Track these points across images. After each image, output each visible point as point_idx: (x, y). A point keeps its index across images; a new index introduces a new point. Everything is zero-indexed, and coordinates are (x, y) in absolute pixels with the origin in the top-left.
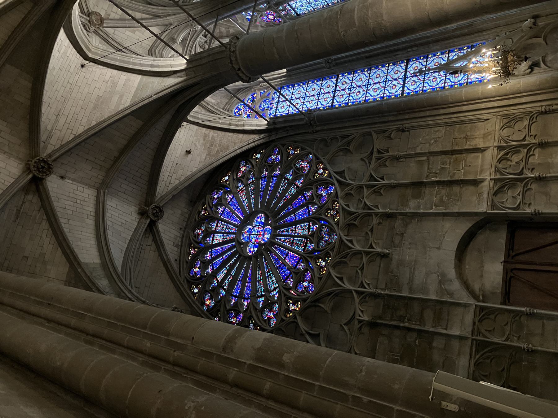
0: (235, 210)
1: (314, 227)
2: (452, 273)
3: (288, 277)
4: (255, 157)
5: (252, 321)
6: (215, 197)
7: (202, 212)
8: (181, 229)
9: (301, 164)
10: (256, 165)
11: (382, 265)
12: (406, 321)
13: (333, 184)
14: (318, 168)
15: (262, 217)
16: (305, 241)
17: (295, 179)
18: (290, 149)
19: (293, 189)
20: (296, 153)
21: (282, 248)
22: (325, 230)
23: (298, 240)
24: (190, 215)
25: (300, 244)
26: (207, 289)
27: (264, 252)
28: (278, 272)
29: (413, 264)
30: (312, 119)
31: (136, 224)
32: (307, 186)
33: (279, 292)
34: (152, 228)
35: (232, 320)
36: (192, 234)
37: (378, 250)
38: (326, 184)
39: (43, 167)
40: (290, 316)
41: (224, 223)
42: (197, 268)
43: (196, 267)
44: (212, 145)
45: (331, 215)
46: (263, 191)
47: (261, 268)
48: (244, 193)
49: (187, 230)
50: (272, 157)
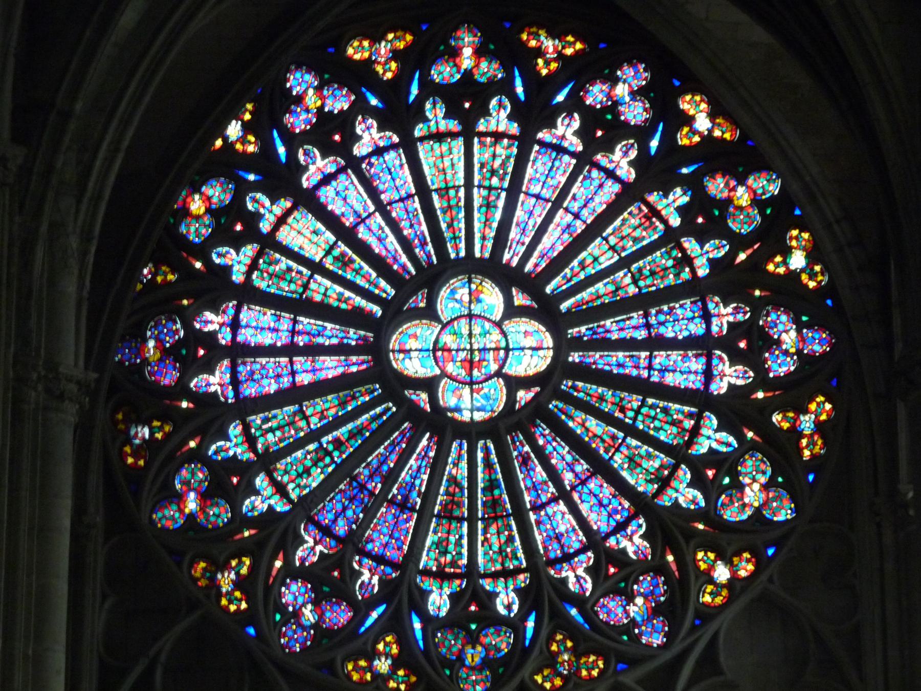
1: (512, 595)
3: (326, 531)
4: (794, 243)
5: (161, 428)
9: (754, 480)
14: (736, 559)
15: (541, 353)
16: (459, 567)
17: (697, 465)
19: (657, 463)
22: (502, 642)
23: (461, 537)
25: (445, 553)
28: (342, 487)
35: (151, 344)
40: (198, 579)
42: (319, 103)
43: (323, 98)
46: (648, 326)
48: (637, 234)
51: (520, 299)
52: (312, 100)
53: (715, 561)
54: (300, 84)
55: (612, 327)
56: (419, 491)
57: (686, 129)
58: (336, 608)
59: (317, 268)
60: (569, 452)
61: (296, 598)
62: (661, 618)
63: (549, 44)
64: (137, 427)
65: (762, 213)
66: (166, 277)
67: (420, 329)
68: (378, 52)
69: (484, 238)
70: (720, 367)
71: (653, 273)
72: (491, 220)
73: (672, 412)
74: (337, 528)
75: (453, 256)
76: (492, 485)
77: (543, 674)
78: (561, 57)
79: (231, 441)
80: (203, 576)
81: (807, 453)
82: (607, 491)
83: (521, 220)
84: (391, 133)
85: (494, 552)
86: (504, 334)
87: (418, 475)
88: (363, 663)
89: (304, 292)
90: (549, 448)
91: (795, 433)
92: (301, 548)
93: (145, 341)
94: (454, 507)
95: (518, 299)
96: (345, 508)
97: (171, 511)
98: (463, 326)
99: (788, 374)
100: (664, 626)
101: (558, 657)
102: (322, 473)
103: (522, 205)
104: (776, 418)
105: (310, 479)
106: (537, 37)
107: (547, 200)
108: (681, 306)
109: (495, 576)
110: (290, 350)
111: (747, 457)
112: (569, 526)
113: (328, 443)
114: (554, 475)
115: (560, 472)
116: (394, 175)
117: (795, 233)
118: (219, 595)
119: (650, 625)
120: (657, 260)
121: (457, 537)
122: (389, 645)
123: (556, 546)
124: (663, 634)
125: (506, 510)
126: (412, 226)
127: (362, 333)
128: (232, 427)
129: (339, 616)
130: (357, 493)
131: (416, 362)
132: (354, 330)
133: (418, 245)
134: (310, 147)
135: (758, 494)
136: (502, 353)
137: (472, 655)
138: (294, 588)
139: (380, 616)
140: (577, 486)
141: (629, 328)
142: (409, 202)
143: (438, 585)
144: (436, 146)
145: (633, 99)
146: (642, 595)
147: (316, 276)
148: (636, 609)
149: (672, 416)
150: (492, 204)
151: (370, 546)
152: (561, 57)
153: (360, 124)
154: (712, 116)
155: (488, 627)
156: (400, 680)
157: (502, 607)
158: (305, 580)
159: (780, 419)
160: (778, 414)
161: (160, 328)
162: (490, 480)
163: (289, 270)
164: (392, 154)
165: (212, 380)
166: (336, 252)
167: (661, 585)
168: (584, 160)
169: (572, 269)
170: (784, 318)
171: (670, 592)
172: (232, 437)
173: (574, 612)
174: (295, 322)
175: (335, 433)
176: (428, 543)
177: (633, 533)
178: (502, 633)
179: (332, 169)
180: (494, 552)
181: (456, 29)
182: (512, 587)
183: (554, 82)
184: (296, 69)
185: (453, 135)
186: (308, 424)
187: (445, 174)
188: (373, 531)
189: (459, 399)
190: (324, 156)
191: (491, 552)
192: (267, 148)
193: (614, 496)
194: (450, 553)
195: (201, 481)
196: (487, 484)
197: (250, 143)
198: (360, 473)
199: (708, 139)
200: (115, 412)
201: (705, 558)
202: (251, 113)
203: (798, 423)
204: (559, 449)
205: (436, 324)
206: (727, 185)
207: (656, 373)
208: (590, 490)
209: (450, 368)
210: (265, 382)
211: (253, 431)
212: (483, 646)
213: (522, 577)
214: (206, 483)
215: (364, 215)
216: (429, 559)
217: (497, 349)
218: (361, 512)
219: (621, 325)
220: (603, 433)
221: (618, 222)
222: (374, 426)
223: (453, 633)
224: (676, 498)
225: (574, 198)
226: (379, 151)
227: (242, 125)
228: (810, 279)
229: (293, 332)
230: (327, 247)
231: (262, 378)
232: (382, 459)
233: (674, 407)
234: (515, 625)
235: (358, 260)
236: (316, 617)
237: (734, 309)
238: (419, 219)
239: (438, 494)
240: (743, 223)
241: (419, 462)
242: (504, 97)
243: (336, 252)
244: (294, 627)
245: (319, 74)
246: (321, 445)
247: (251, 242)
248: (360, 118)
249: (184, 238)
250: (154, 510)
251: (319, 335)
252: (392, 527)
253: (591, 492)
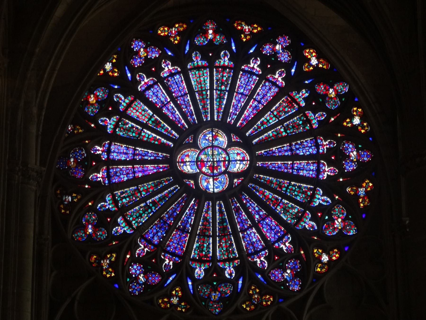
0: (255, 100)
1: (232, 269)
3: (149, 242)
4: (355, 113)
5: (76, 197)
6: (278, 47)
7: (247, 28)
9: (339, 217)
14: (331, 252)
15: (244, 162)
17: (314, 211)
18: (369, 186)
20: (361, 200)
21: (193, 218)
22: (228, 290)
23: (209, 244)
28: (156, 222)
35: (72, 160)
40: (93, 263)
41: (230, 82)
42: (145, 54)
43: (147, 52)
46: (291, 150)
50: (352, 152)
51: (234, 139)
53: (322, 253)
54: (137, 47)
55: (276, 150)
56: (190, 224)
57: (307, 64)
58: (153, 276)
59: (145, 126)
60: (257, 206)
61: (136, 271)
62: (298, 279)
63: (246, 28)
64: (66, 197)
65: (341, 100)
66: (78, 131)
67: (190, 153)
68: (171, 32)
69: (218, 112)
70: (323, 168)
71: (293, 127)
72: (221, 104)
73: (303, 188)
74: (154, 241)
75: (205, 120)
76: (223, 221)
77: (246, 304)
78: (251, 33)
79: (107, 202)
80: (95, 261)
81: (362, 205)
83: (235, 104)
84: (177, 67)
85: (224, 251)
86: (228, 154)
87: (190, 217)
88: (166, 300)
89: (139, 137)
90: (248, 204)
91: (356, 196)
92: (138, 250)
93: (70, 158)
94: (206, 231)
95: (234, 139)
96: (157, 232)
97: (81, 234)
98: (209, 151)
99: (353, 170)
100: (299, 282)
101: (253, 296)
102: (147, 216)
103: (235, 98)
104: (348, 189)
105: (142, 219)
106: (241, 25)
107: (246, 96)
108: (306, 141)
109: (224, 261)
110: (133, 162)
111: (335, 207)
112: (257, 239)
113: (150, 203)
114: (251, 217)
115: (253, 215)
116: (179, 85)
117: (355, 109)
118: (102, 270)
119: (293, 282)
120: (295, 121)
121: (207, 244)
122: (177, 291)
123: (251, 247)
124: (299, 285)
125: (229, 232)
126: (186, 107)
127: (165, 154)
128: (107, 196)
129: (155, 279)
130: (163, 225)
131: (189, 167)
132: (161, 153)
133: (189, 115)
134: (142, 74)
135: (340, 223)
136: (227, 162)
137: (214, 296)
138: (135, 267)
139: (173, 279)
140: (261, 221)
141: (283, 151)
142: (185, 97)
143: (199, 265)
144: (197, 72)
145: (283, 51)
146: (290, 268)
147: (144, 130)
148: (287, 275)
149: (303, 189)
150: (222, 97)
151: (169, 249)
152: (251, 33)
153: (163, 63)
154: (318, 58)
155: (221, 283)
156: (182, 307)
157: (228, 275)
159: (350, 190)
160: (349, 188)
161: (76, 153)
162: (222, 219)
163: (133, 127)
164: (178, 76)
165: (99, 175)
166: (153, 119)
167: (298, 264)
168: (262, 78)
169: (257, 126)
170: (351, 146)
171: (302, 267)
172: (108, 201)
173: (259, 276)
174: (135, 150)
175: (153, 199)
176: (195, 247)
177: (286, 241)
178: (228, 286)
179: (151, 83)
180: (224, 251)
181: (206, 22)
182: (232, 266)
183: (249, 44)
184: (136, 40)
185: (204, 67)
186: (141, 195)
187: (201, 84)
188: (170, 241)
189: (208, 183)
191: (222, 251)
192: (123, 75)
193: (277, 225)
194: (205, 251)
195: (94, 220)
196: (221, 220)
197: (116, 72)
198: (164, 216)
199: (316, 67)
200: (56, 190)
201: (318, 252)
202: (116, 59)
203: (358, 192)
204: (253, 205)
205: (197, 150)
206: (325, 88)
207: (295, 171)
208: (266, 223)
209: (204, 169)
210: (122, 176)
211: (117, 198)
212: (219, 292)
213: (236, 261)
214: (96, 221)
215: (165, 103)
216: (195, 254)
217: (224, 161)
218: (165, 233)
219: (280, 149)
220: (272, 198)
221: (277, 105)
222: (170, 195)
223: (205, 286)
224: (305, 226)
225: (258, 95)
226: (172, 75)
227: (112, 65)
228: (362, 129)
229: (134, 154)
230: (149, 117)
231: (121, 175)
232: (174, 210)
234: (234, 282)
235: (163, 122)
236: (145, 280)
237: (329, 142)
238: (190, 104)
239: (199, 225)
240: (332, 105)
241: (190, 211)
242: (226, 51)
243: (153, 119)
244: (135, 284)
245: (145, 42)
246: (147, 204)
247: (116, 115)
248: (163, 61)
249: (87, 113)
250: (73, 233)
251: (145, 156)
252: (178, 240)
253: (267, 224)
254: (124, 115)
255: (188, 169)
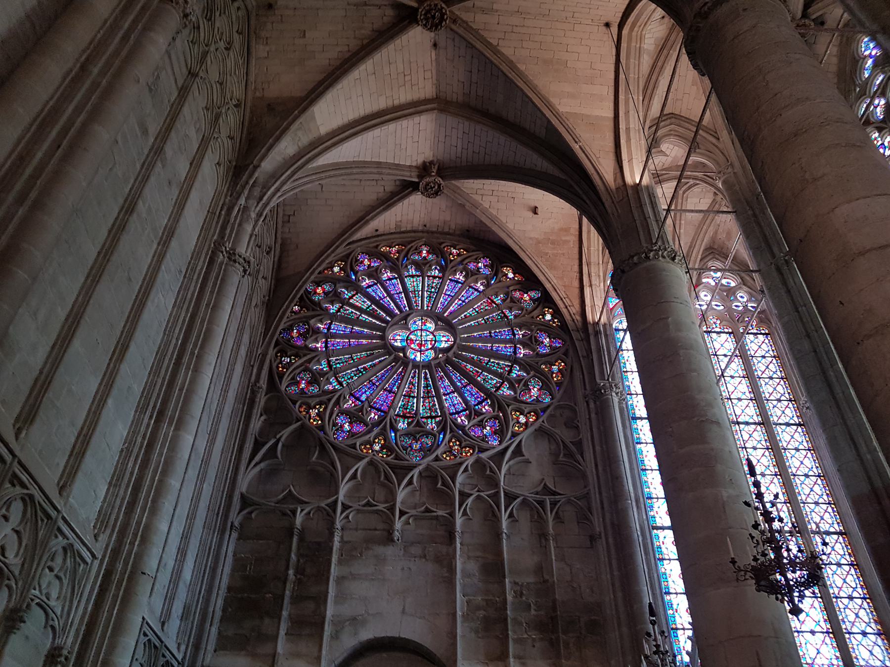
0: (460, 300)
2: (366, 634)
5: (294, 359)
6: (480, 265)
8: (425, 226)
10: (533, 317)
11: (377, 532)
12: (298, 577)
13: (501, 442)
14: (528, 415)
19: (495, 382)
22: (428, 441)
24: (448, 234)
25: (407, 409)
26: (338, 285)
27: (393, 356)
29: (380, 577)
30: (603, 391)
31: (408, 164)
32: (499, 404)
33: (335, 391)
34: (406, 188)
35: (295, 331)
36: (420, 244)
37: (398, 525)
38: (500, 433)
39: (433, 17)
43: (370, 262)
44: (553, 243)
45: (451, 447)
46: (491, 336)
47: (371, 358)
49: (425, 234)
52: (366, 262)
69: (428, 306)
76: (427, 386)
81: (555, 379)
82: (475, 390)
88: (368, 446)
93: (293, 330)
96: (366, 391)
98: (419, 333)
109: (427, 418)
154: (514, 274)
158: (347, 415)
163: (352, 312)
166: (371, 308)
185: (418, 276)
190: (369, 279)
192: (349, 276)
217: (432, 341)
221: (479, 304)
229: (351, 332)
233: (502, 362)
243: (371, 308)
253: (468, 390)
254: (345, 302)
255: (398, 344)
